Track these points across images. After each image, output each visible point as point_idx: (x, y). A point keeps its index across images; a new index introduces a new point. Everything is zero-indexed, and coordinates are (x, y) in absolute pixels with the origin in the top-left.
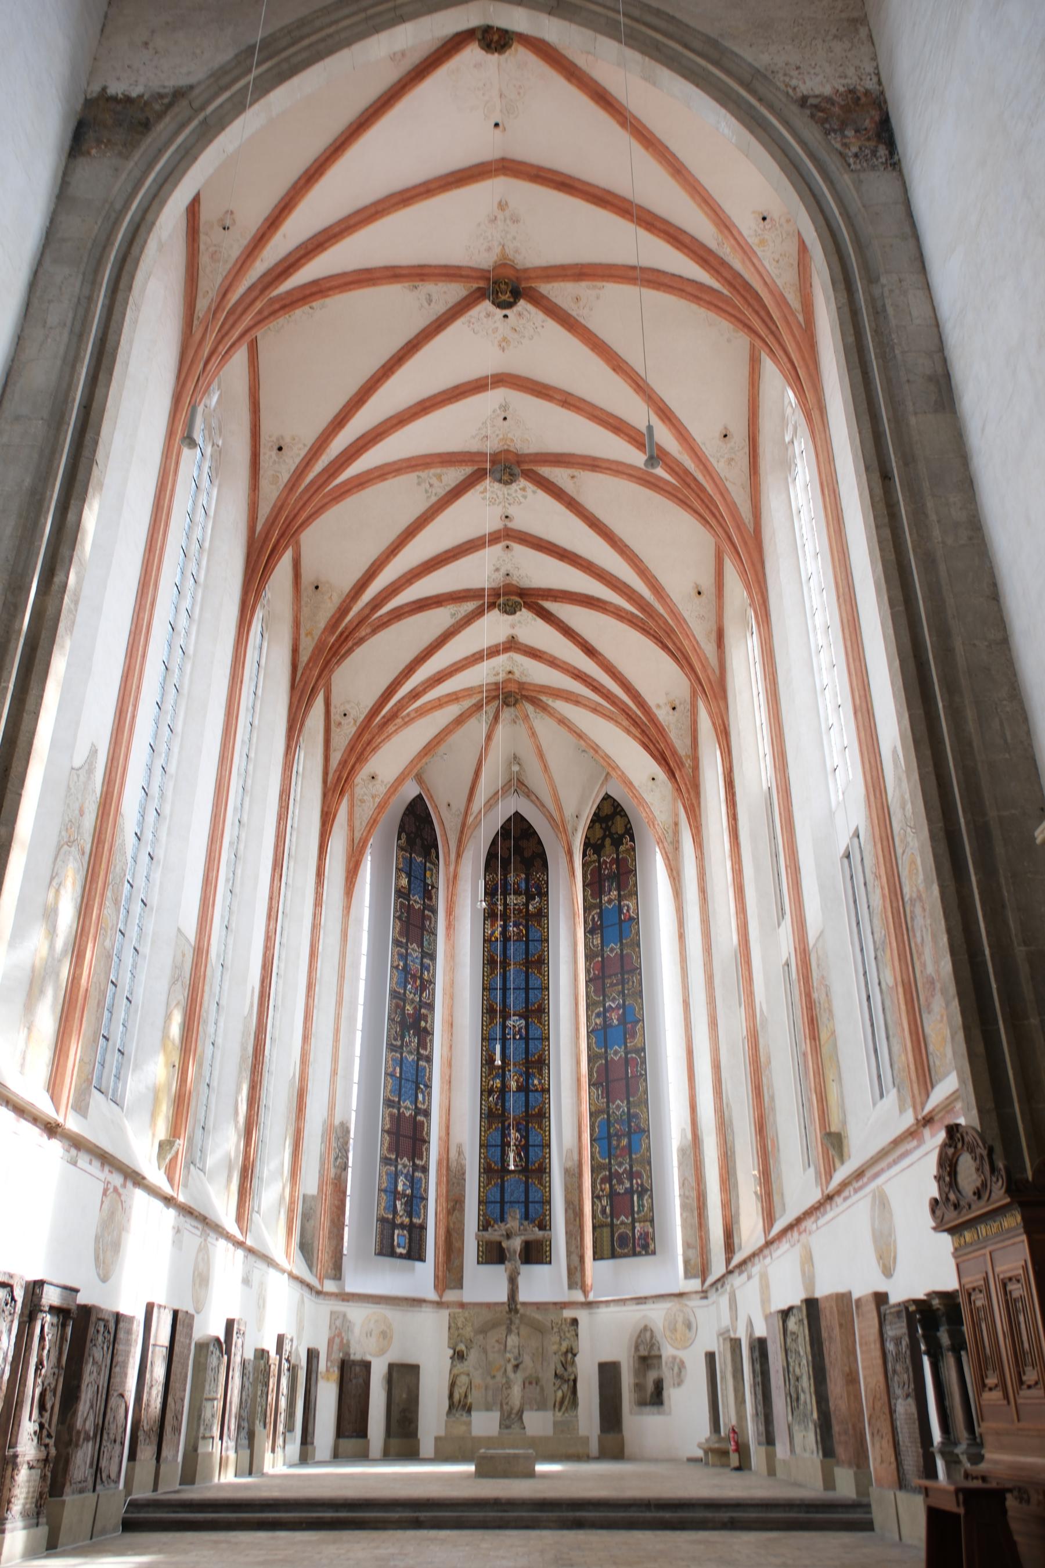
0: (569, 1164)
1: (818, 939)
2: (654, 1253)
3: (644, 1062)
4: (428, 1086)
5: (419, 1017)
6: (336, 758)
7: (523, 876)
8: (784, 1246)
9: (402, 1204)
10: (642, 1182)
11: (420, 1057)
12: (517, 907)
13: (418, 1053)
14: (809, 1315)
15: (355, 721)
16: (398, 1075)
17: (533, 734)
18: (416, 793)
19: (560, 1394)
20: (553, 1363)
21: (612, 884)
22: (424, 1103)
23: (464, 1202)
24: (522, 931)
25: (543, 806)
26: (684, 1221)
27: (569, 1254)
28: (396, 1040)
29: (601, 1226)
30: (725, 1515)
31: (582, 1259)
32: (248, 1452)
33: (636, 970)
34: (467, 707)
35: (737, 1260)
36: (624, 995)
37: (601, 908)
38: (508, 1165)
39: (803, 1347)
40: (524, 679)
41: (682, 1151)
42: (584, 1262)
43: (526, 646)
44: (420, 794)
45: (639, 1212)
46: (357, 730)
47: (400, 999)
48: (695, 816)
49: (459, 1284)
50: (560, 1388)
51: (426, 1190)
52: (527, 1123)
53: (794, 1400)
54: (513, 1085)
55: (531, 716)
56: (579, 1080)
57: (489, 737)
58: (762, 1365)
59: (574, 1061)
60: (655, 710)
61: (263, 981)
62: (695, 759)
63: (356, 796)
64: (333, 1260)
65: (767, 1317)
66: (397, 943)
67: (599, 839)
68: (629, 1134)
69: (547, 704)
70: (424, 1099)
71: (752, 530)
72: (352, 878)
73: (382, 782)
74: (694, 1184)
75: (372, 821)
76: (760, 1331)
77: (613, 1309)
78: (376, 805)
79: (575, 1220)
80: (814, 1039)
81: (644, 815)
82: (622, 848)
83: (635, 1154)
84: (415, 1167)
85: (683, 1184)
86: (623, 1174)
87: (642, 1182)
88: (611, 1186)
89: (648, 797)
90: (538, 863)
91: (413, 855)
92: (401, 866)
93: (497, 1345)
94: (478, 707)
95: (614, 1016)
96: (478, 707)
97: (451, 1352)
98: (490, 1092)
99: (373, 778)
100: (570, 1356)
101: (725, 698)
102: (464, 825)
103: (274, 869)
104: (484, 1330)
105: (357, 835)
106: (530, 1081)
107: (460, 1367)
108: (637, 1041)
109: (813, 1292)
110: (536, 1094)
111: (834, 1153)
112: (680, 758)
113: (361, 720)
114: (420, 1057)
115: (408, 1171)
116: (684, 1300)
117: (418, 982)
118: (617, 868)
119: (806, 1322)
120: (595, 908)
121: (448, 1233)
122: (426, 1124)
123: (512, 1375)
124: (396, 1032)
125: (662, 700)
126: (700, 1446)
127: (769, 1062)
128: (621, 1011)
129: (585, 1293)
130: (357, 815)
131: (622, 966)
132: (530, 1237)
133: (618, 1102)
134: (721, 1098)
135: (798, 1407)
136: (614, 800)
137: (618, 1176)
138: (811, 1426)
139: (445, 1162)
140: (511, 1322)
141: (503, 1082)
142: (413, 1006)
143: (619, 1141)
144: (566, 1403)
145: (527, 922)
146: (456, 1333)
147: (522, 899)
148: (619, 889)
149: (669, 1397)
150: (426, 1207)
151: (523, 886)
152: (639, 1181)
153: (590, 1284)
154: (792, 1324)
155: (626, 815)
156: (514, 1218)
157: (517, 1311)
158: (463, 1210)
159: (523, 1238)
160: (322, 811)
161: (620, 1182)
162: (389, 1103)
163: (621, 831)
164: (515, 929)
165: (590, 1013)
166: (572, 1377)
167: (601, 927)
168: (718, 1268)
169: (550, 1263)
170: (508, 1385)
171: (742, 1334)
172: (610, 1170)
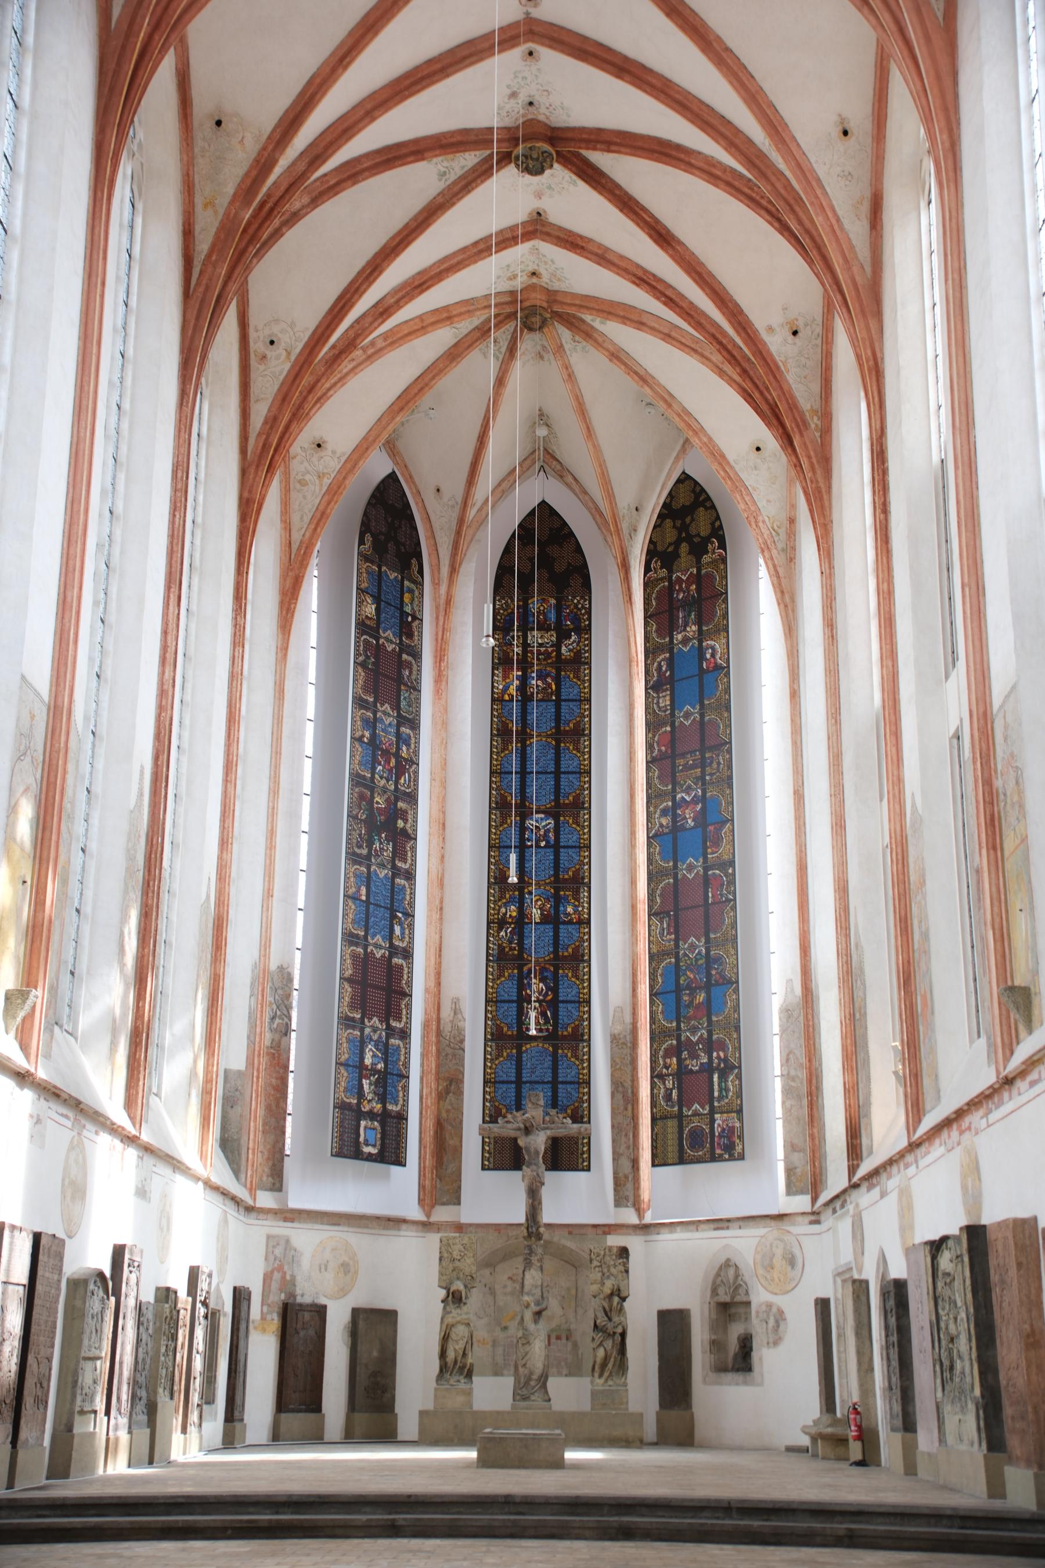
0: (618, 1029)
1: (1008, 696)
2: (742, 1157)
3: (732, 882)
4: (410, 915)
5: (394, 814)
6: (259, 412)
7: (553, 601)
8: (937, 1150)
9: (370, 1084)
10: (726, 1057)
11: (396, 872)
12: (543, 649)
13: (394, 866)
14: (970, 1250)
15: (289, 354)
16: (364, 898)
17: (570, 377)
18: (390, 471)
19: (601, 1353)
20: (592, 1309)
21: (690, 616)
22: (402, 940)
23: (462, 1082)
24: (550, 685)
25: (585, 492)
26: (787, 1111)
27: (616, 1156)
28: (360, 847)
29: (664, 1118)
30: (841, 1527)
31: (635, 1163)
32: (148, 1431)
33: (724, 745)
34: (465, 331)
35: (863, 1170)
36: (704, 783)
37: (671, 651)
38: (528, 1029)
39: (961, 1294)
40: (556, 286)
41: (787, 1012)
42: (638, 1169)
43: (560, 228)
44: (394, 472)
45: (720, 1098)
46: (293, 366)
47: (366, 786)
48: (822, 507)
49: (455, 1198)
50: (601, 1344)
51: (407, 1065)
52: (557, 968)
53: (946, 1369)
54: (536, 914)
55: (567, 347)
56: (634, 907)
57: (500, 382)
58: (898, 1319)
59: (627, 879)
60: (765, 336)
61: (156, 758)
62: (826, 416)
63: (293, 474)
64: (271, 1163)
65: (909, 1251)
66: (360, 703)
67: (670, 544)
68: (708, 987)
69: (592, 327)
70: (403, 933)
71: (940, 15)
72: (290, 604)
73: (334, 452)
74: (803, 1060)
75: (318, 515)
76: (898, 1270)
77: (679, 1235)
78: (325, 489)
79: (626, 1109)
80: (994, 848)
81: (742, 506)
82: (706, 559)
83: (717, 1015)
84: (390, 1031)
85: (788, 1060)
86: (697, 1043)
87: (726, 1057)
88: (680, 1061)
89: (749, 479)
90: (576, 581)
91: (384, 568)
92: (364, 585)
93: (509, 1283)
94: (482, 332)
95: (689, 814)
96: (482, 332)
97: (443, 1293)
98: (502, 923)
99: (319, 446)
100: (616, 1299)
101: (878, 313)
102: (461, 521)
103: (168, 588)
104: (490, 1263)
105: (297, 537)
106: (562, 908)
107: (456, 1314)
108: (723, 850)
109: (979, 1217)
110: (570, 928)
111: (1017, 1016)
112: (802, 414)
113: (298, 350)
114: (396, 872)
115: (380, 1037)
116: (786, 1226)
117: (393, 761)
118: (698, 590)
119: (966, 1259)
120: (663, 652)
121: (439, 1125)
122: (406, 970)
123: (531, 1327)
124: (360, 835)
125: (776, 319)
126: (805, 1430)
127: (922, 883)
128: (699, 807)
129: (640, 1212)
130: (295, 505)
131: (702, 740)
132: (560, 1132)
133: (692, 939)
134: (848, 936)
135: (951, 1379)
136: (696, 483)
137: (690, 1045)
138: (971, 1407)
139: (434, 1024)
140: (531, 1252)
141: (521, 910)
142: (386, 796)
143: (692, 996)
144: (610, 1366)
145: (559, 671)
146: (451, 1268)
147: (552, 637)
148: (700, 623)
149: (761, 1359)
150: (406, 1089)
151: (553, 616)
152: (722, 1054)
153: (646, 1200)
154: (945, 1261)
155: (713, 507)
156: (536, 1105)
157: (539, 1236)
158: (462, 1093)
159: (549, 1132)
160: (241, 498)
161: (694, 1056)
162: (350, 938)
163: (704, 531)
164: (540, 683)
165: (652, 809)
166: (619, 1330)
167: (671, 680)
168: (836, 1179)
169: (588, 1169)
170: (526, 1340)
171: (870, 1273)
172: (678, 1038)
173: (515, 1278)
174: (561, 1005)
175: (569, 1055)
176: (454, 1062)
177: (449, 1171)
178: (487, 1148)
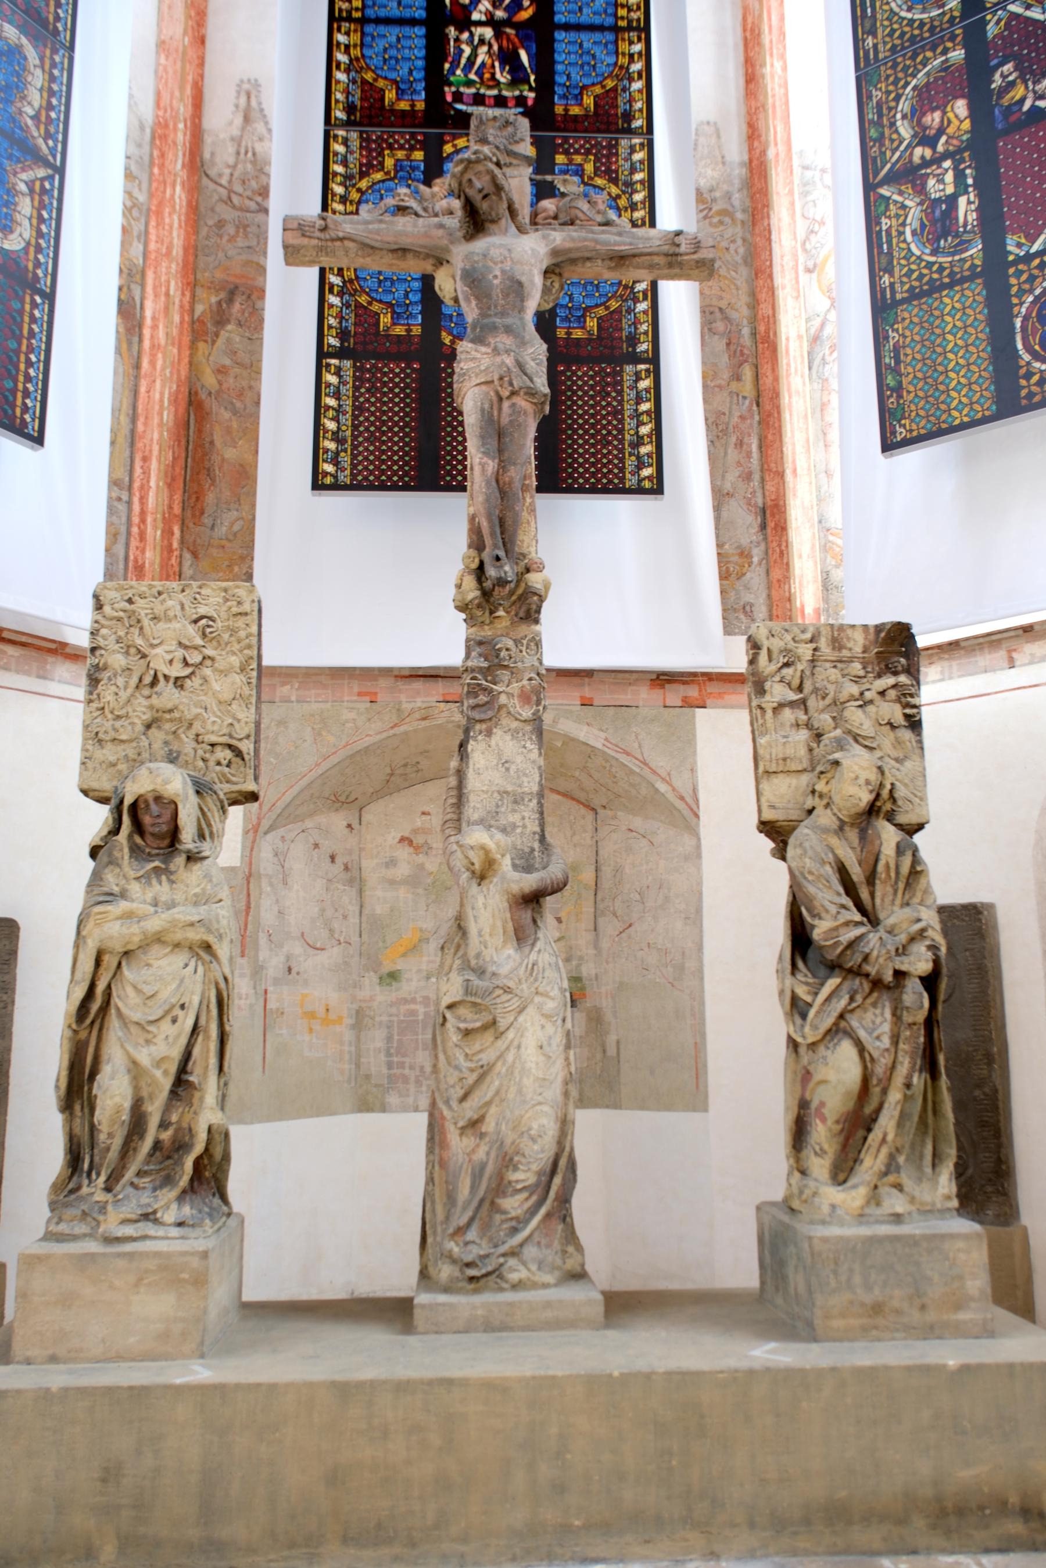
0: (709, 175)
42: (782, 528)
50: (838, 1030)
93: (404, 853)
97: (99, 816)
100: (888, 835)
144: (887, 1123)
146: (141, 710)
158: (258, 325)
173: (419, 840)
174: (560, 35)
175: (589, 168)
176: (241, 242)
177: (222, 530)
178: (331, 425)
